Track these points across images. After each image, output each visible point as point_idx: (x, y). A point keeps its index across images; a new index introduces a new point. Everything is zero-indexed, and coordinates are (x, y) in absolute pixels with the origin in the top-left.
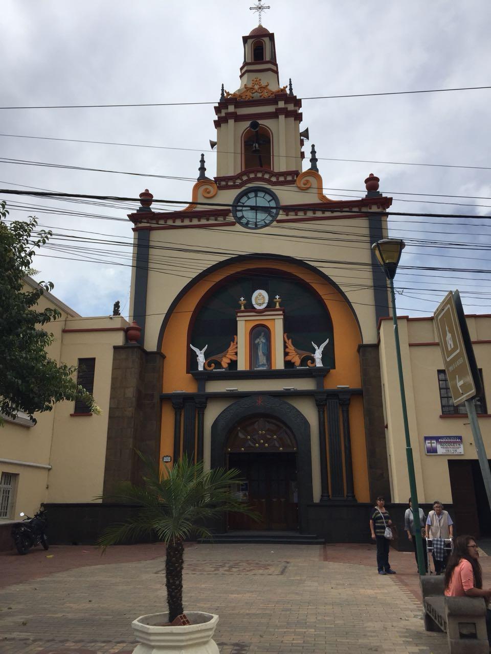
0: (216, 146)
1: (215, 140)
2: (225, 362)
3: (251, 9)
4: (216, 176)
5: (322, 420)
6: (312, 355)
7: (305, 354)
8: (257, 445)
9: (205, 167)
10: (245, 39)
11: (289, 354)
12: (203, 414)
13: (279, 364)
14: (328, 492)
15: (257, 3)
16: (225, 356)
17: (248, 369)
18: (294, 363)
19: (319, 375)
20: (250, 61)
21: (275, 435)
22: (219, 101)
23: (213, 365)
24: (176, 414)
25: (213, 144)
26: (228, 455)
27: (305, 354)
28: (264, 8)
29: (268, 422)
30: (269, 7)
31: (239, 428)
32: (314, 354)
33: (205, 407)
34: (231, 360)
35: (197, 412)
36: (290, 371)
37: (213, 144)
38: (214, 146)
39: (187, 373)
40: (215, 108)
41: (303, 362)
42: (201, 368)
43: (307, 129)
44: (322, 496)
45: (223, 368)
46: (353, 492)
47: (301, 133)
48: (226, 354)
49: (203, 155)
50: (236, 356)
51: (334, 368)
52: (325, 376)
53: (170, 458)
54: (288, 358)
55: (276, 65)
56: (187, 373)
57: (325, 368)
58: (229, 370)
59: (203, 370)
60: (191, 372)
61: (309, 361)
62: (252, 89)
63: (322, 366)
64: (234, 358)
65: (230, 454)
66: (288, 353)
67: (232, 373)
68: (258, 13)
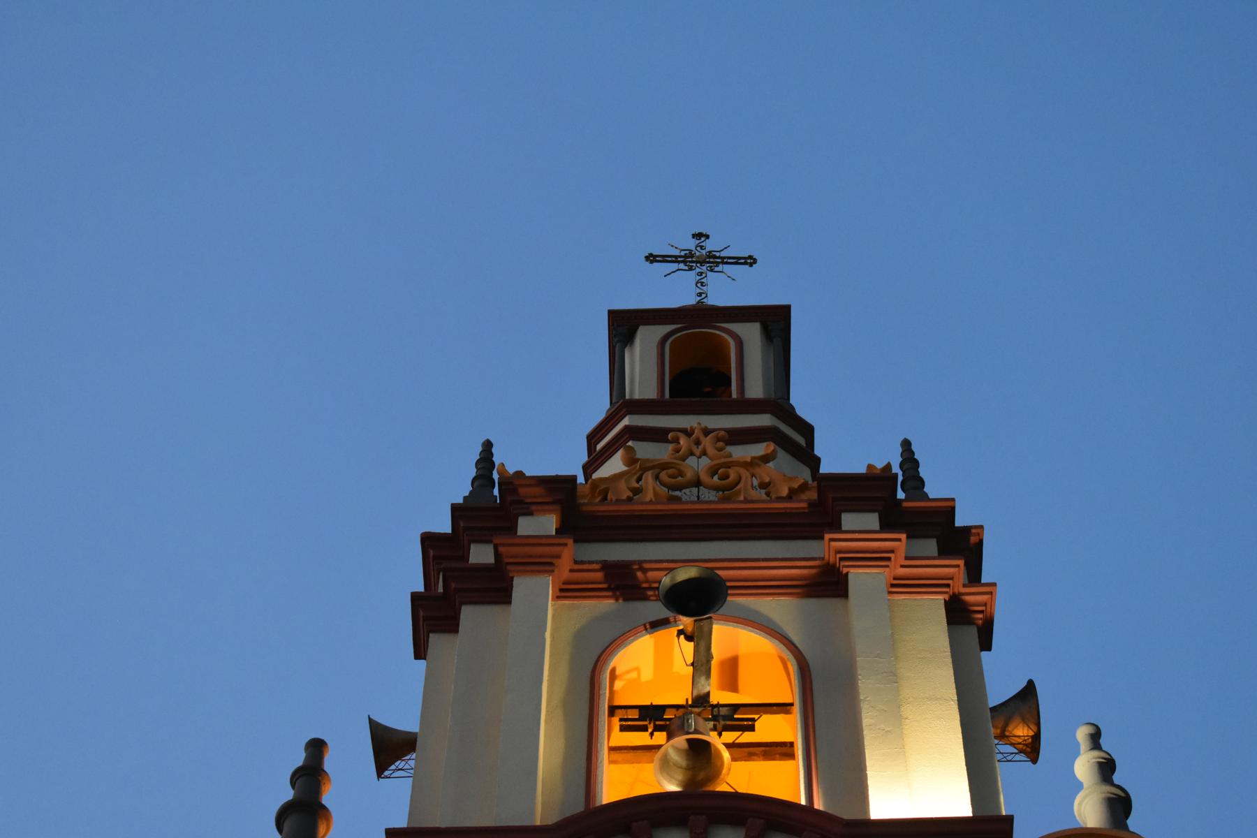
0: (410, 762)
1: (405, 720)
3: (651, 258)
4: (402, 822)
9: (327, 799)
10: (623, 326)
15: (691, 244)
20: (651, 393)
22: (461, 501)
25: (389, 747)
28: (725, 261)
30: (750, 261)
37: (389, 747)
38: (399, 757)
40: (429, 540)
43: (1028, 693)
47: (993, 709)
49: (316, 747)
55: (807, 430)
62: (664, 466)
68: (692, 276)
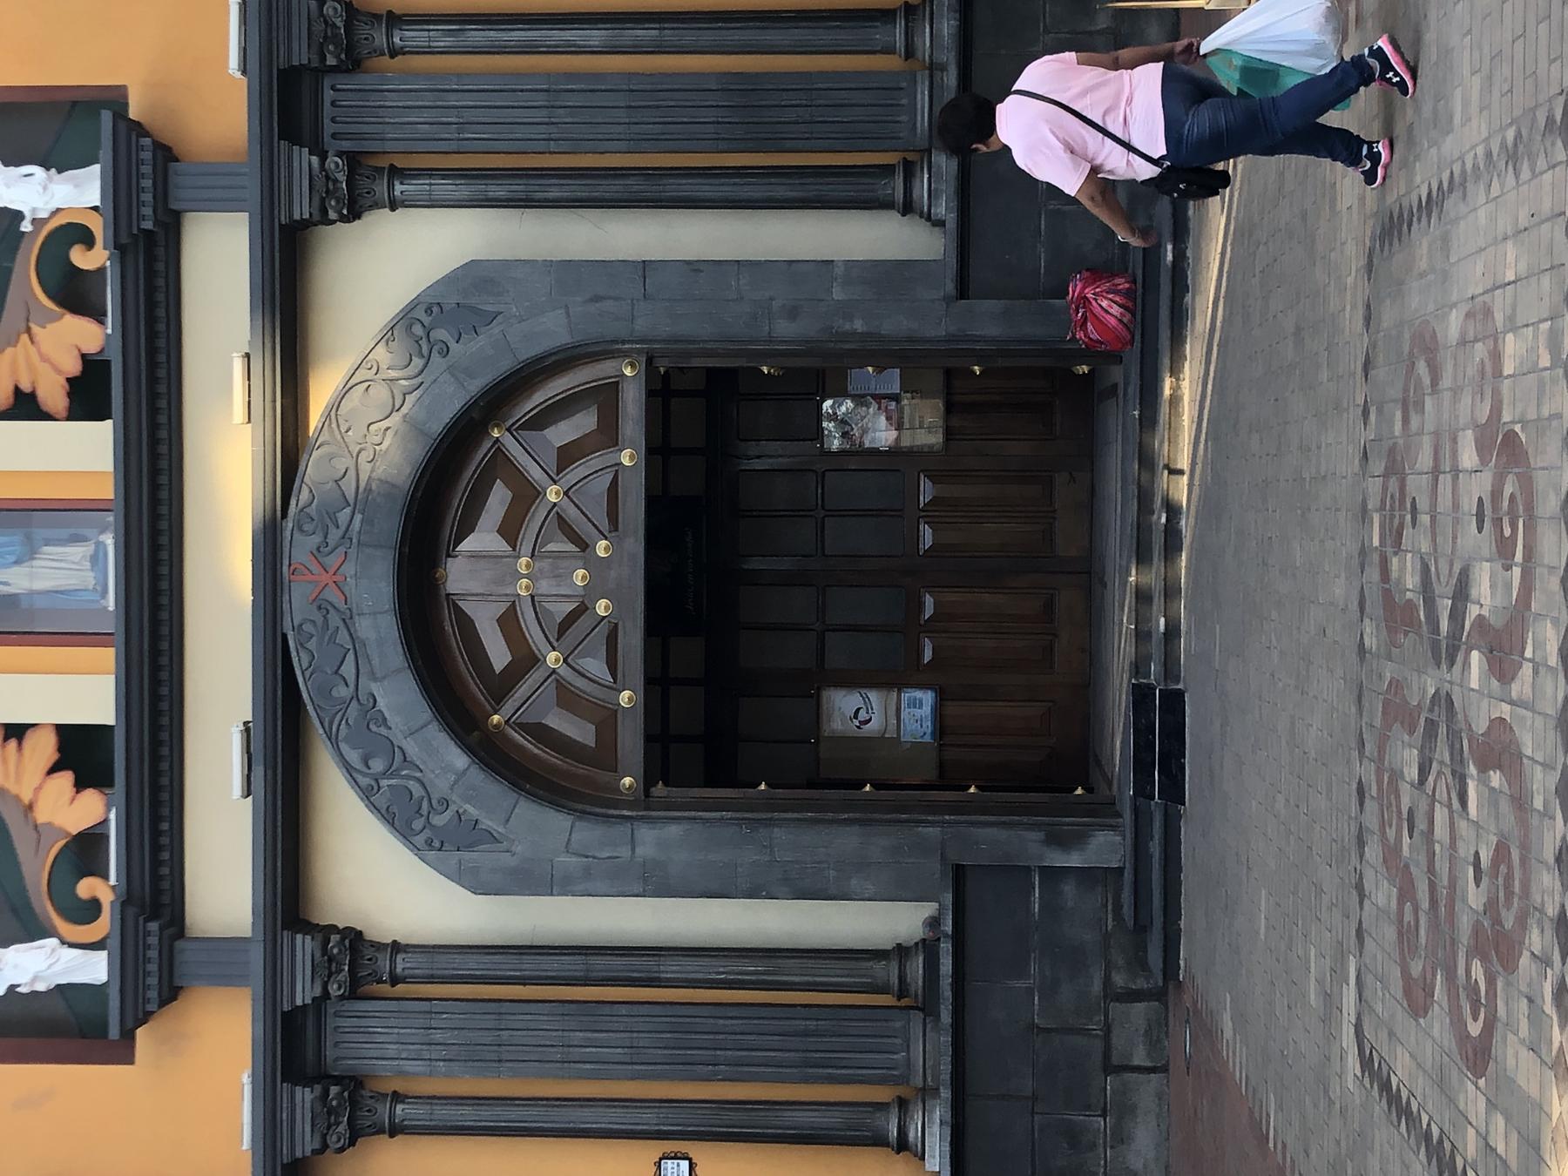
2: (72, 809)
5: (444, 188)
6: (26, 227)
7: (27, 280)
8: (602, 607)
11: (26, 387)
12: (396, 947)
13: (84, 453)
14: (888, 170)
16: (30, 807)
17: (108, 656)
18: (83, 356)
19: (153, 187)
21: (537, 494)
23: (87, 887)
24: (395, 1130)
26: (659, 789)
27: (27, 280)
29: (467, 527)
31: (496, 718)
32: (18, 216)
33: (354, 938)
34: (54, 769)
35: (385, 989)
36: (138, 392)
39: (129, 1059)
41: (75, 294)
42: (94, 969)
44: (907, 208)
45: (106, 821)
46: (886, 15)
48: (17, 798)
50: (30, 739)
51: (114, 100)
52: (166, 155)
53: (669, 1165)
54: (53, 394)
56: (132, 1063)
57: (106, 151)
58: (111, 784)
59: (104, 954)
60: (114, 1032)
61: (82, 259)
63: (96, 168)
64: (44, 748)
65: (648, 782)
66: (17, 391)
67: (134, 757)
